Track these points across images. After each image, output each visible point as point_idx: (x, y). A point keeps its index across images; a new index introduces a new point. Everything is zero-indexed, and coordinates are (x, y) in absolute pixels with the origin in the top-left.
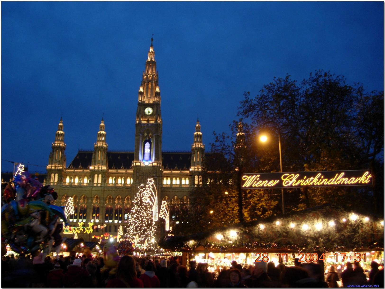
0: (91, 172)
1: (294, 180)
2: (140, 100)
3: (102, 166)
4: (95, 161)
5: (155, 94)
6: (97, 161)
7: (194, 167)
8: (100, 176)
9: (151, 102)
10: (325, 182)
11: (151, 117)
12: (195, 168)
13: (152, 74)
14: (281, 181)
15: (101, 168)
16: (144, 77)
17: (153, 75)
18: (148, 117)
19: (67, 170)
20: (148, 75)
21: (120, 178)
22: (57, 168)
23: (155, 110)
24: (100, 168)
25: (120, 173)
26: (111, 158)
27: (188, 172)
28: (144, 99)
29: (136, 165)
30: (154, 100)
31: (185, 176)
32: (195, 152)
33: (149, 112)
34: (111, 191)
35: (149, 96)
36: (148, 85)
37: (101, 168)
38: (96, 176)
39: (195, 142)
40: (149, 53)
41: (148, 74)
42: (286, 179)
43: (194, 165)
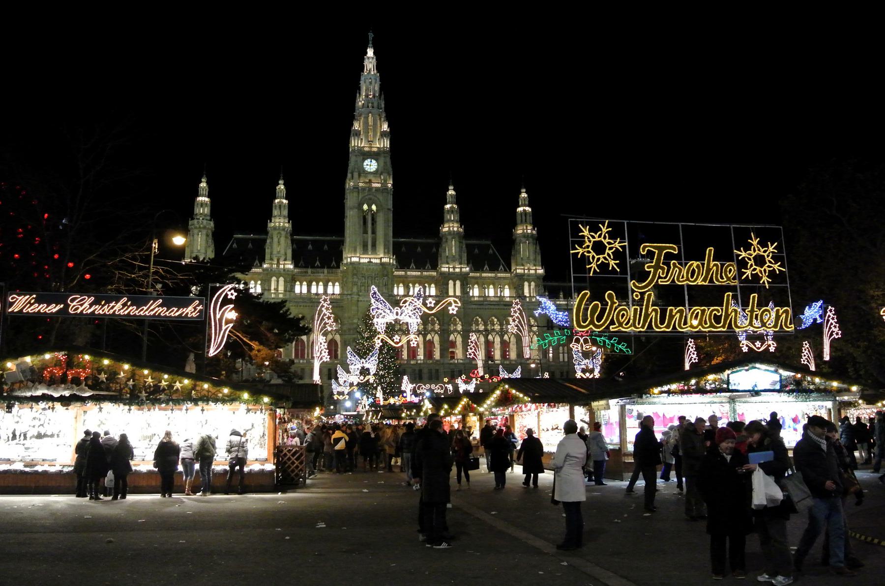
0: (266, 272)
2: (356, 145)
3: (286, 262)
4: (271, 254)
6: (275, 252)
7: (447, 266)
8: (281, 280)
9: (375, 150)
11: (375, 177)
12: (449, 268)
15: (284, 267)
21: (314, 283)
23: (382, 164)
24: (282, 266)
26: (311, 248)
27: (434, 274)
30: (378, 146)
31: (431, 280)
32: (447, 239)
34: (302, 307)
36: (367, 118)
37: (284, 267)
39: (449, 221)
43: (448, 263)
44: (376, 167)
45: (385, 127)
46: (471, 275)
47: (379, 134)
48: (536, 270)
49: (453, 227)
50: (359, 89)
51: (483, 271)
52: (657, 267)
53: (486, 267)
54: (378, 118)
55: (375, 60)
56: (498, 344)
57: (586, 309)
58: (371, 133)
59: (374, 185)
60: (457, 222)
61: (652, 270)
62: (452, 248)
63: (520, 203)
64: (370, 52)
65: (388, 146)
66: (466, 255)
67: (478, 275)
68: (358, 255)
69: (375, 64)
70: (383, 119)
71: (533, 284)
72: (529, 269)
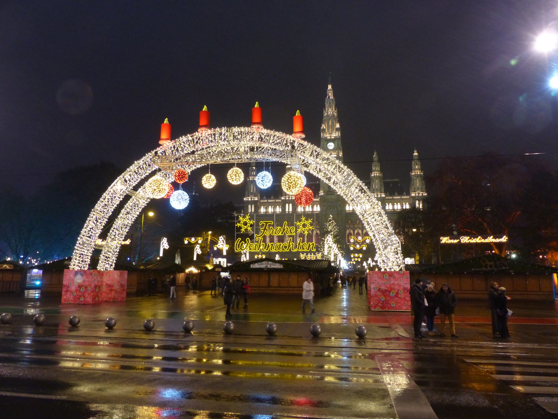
1: (467, 240)
5: (336, 130)
8: (291, 205)
9: (333, 138)
10: (483, 241)
11: (333, 151)
14: (460, 240)
17: (333, 113)
19: (262, 201)
22: (253, 199)
23: (337, 145)
24: (290, 198)
28: (326, 135)
30: (335, 136)
38: (287, 205)
39: (374, 171)
40: (328, 91)
42: (463, 239)
45: (338, 126)
49: (377, 174)
50: (325, 107)
51: (394, 195)
52: (265, 229)
53: (396, 193)
54: (334, 121)
55: (332, 91)
57: (239, 244)
60: (378, 171)
61: (263, 230)
64: (330, 87)
66: (383, 188)
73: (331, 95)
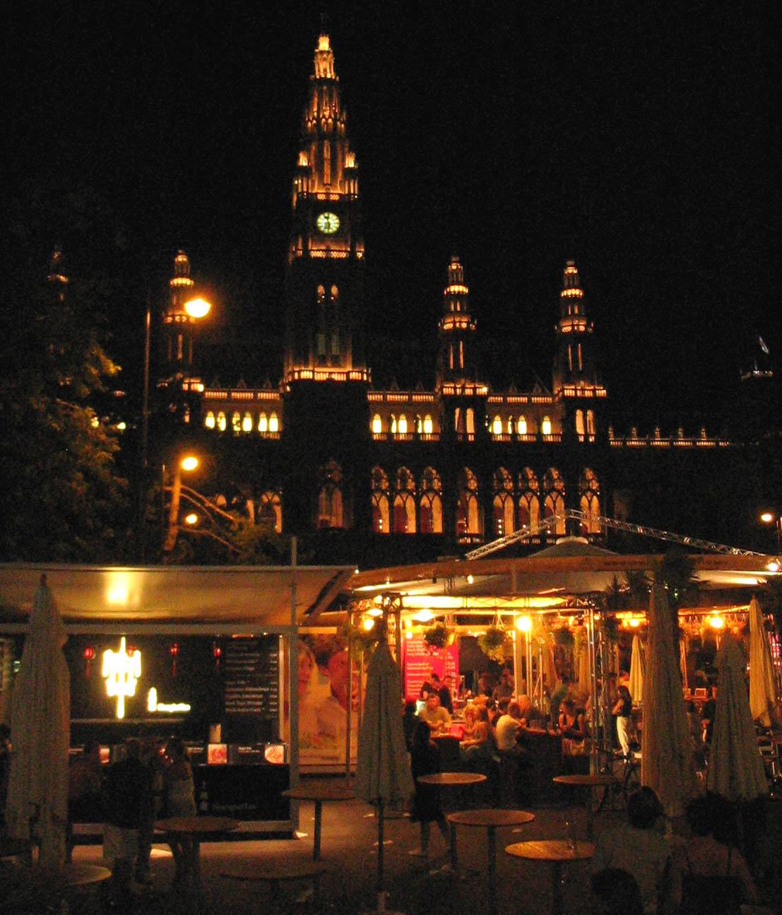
2: (305, 190)
3: (192, 381)
9: (336, 198)
12: (455, 388)
13: (333, 116)
16: (310, 124)
17: (335, 120)
18: (326, 238)
20: (321, 119)
25: (236, 400)
27: (431, 398)
29: (302, 377)
30: (343, 193)
31: (424, 409)
33: (328, 226)
35: (327, 180)
40: (319, 56)
41: (321, 116)
44: (337, 226)
45: (350, 163)
46: (491, 399)
47: (340, 174)
48: (594, 391)
49: (460, 322)
55: (331, 56)
56: (534, 512)
58: (327, 169)
59: (334, 255)
62: (458, 356)
63: (566, 283)
64: (324, 44)
65: (356, 193)
67: (500, 399)
68: (311, 368)
69: (333, 62)
70: (347, 149)
71: (590, 413)
72: (583, 390)
73: (325, 68)
